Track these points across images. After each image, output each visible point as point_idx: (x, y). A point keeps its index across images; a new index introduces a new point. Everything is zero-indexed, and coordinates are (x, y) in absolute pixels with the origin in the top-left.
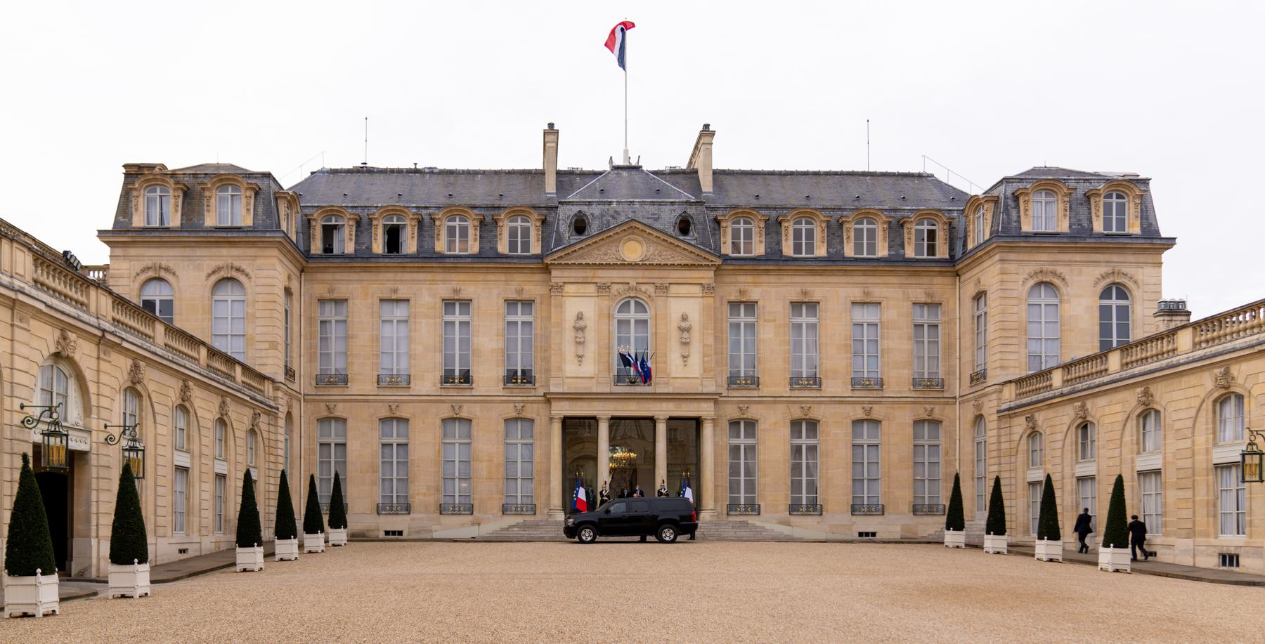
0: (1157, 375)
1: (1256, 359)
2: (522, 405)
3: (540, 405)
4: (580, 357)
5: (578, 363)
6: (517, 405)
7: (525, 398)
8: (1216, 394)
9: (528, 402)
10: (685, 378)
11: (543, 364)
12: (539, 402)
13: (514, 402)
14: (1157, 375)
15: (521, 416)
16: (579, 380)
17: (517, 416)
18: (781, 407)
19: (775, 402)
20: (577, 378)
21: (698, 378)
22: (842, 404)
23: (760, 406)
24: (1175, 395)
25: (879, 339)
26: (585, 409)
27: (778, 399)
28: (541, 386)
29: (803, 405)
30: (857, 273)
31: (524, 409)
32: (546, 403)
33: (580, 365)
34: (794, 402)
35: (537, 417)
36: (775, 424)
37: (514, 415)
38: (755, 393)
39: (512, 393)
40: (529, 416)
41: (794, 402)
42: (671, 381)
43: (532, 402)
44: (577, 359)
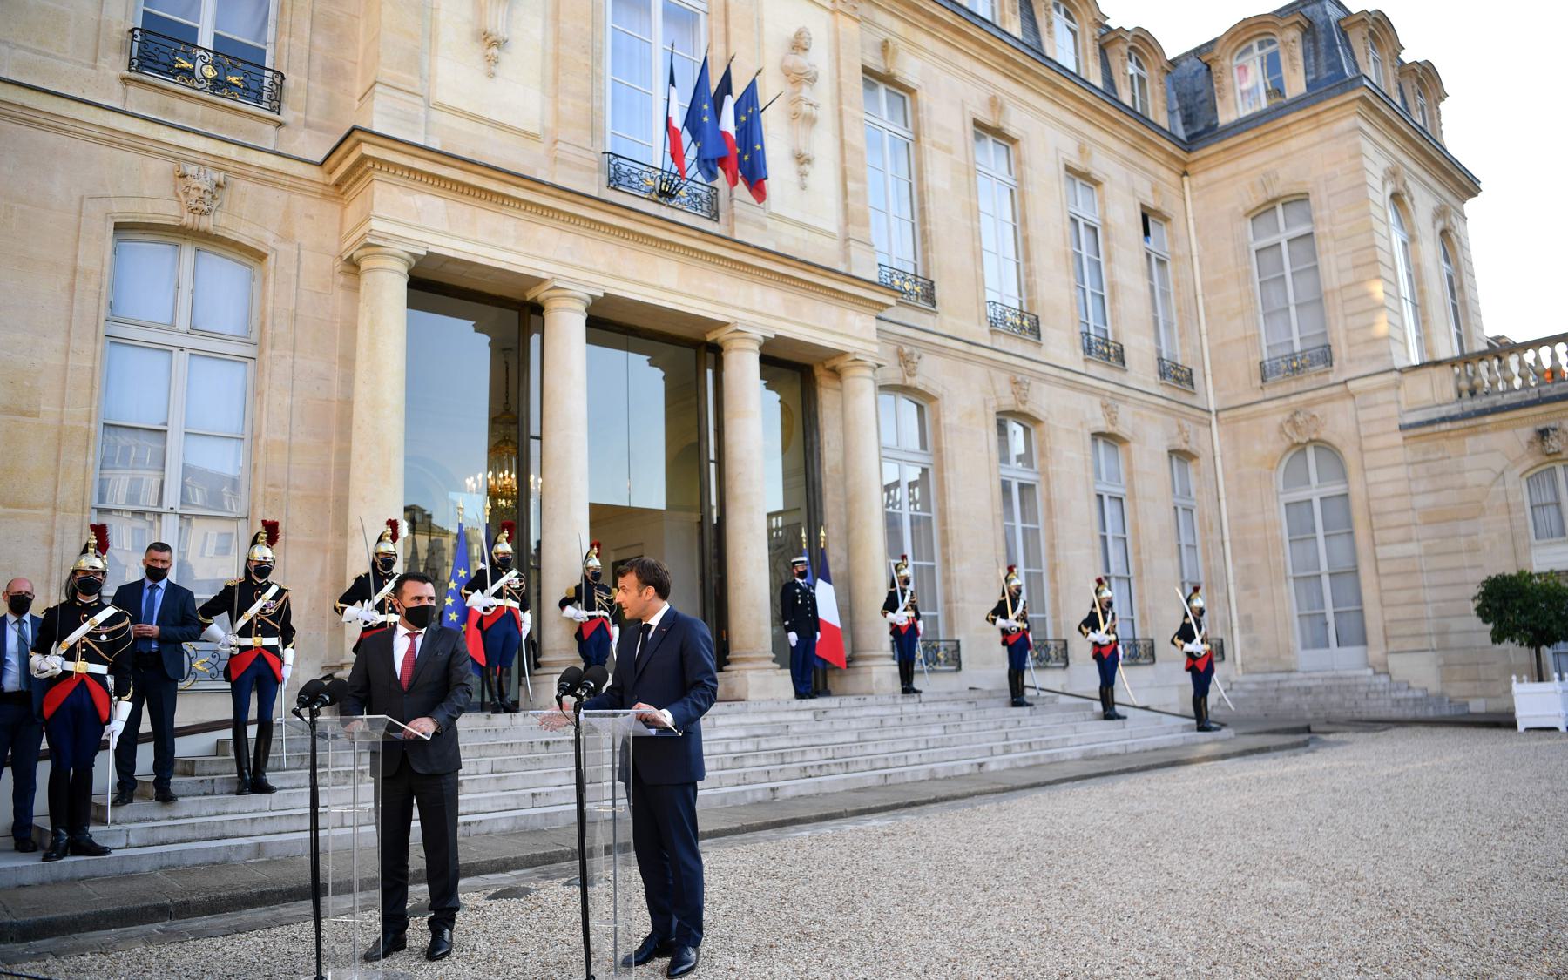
2: (219, 177)
3: (299, 201)
4: (491, 43)
6: (192, 170)
7: (233, 152)
9: (242, 171)
10: (804, 226)
11: (319, 41)
12: (294, 185)
13: (178, 155)
15: (206, 223)
16: (484, 130)
17: (188, 220)
18: (978, 372)
19: (968, 358)
20: (478, 119)
22: (1073, 388)
23: (939, 362)
25: (1102, 259)
26: (510, 245)
27: (975, 350)
28: (307, 125)
31: (225, 195)
33: (492, 75)
34: (1000, 366)
35: (282, 247)
36: (971, 415)
37: (168, 211)
38: (927, 321)
39: (173, 112)
40: (243, 233)
41: (1000, 366)
42: (770, 223)
43: (266, 178)
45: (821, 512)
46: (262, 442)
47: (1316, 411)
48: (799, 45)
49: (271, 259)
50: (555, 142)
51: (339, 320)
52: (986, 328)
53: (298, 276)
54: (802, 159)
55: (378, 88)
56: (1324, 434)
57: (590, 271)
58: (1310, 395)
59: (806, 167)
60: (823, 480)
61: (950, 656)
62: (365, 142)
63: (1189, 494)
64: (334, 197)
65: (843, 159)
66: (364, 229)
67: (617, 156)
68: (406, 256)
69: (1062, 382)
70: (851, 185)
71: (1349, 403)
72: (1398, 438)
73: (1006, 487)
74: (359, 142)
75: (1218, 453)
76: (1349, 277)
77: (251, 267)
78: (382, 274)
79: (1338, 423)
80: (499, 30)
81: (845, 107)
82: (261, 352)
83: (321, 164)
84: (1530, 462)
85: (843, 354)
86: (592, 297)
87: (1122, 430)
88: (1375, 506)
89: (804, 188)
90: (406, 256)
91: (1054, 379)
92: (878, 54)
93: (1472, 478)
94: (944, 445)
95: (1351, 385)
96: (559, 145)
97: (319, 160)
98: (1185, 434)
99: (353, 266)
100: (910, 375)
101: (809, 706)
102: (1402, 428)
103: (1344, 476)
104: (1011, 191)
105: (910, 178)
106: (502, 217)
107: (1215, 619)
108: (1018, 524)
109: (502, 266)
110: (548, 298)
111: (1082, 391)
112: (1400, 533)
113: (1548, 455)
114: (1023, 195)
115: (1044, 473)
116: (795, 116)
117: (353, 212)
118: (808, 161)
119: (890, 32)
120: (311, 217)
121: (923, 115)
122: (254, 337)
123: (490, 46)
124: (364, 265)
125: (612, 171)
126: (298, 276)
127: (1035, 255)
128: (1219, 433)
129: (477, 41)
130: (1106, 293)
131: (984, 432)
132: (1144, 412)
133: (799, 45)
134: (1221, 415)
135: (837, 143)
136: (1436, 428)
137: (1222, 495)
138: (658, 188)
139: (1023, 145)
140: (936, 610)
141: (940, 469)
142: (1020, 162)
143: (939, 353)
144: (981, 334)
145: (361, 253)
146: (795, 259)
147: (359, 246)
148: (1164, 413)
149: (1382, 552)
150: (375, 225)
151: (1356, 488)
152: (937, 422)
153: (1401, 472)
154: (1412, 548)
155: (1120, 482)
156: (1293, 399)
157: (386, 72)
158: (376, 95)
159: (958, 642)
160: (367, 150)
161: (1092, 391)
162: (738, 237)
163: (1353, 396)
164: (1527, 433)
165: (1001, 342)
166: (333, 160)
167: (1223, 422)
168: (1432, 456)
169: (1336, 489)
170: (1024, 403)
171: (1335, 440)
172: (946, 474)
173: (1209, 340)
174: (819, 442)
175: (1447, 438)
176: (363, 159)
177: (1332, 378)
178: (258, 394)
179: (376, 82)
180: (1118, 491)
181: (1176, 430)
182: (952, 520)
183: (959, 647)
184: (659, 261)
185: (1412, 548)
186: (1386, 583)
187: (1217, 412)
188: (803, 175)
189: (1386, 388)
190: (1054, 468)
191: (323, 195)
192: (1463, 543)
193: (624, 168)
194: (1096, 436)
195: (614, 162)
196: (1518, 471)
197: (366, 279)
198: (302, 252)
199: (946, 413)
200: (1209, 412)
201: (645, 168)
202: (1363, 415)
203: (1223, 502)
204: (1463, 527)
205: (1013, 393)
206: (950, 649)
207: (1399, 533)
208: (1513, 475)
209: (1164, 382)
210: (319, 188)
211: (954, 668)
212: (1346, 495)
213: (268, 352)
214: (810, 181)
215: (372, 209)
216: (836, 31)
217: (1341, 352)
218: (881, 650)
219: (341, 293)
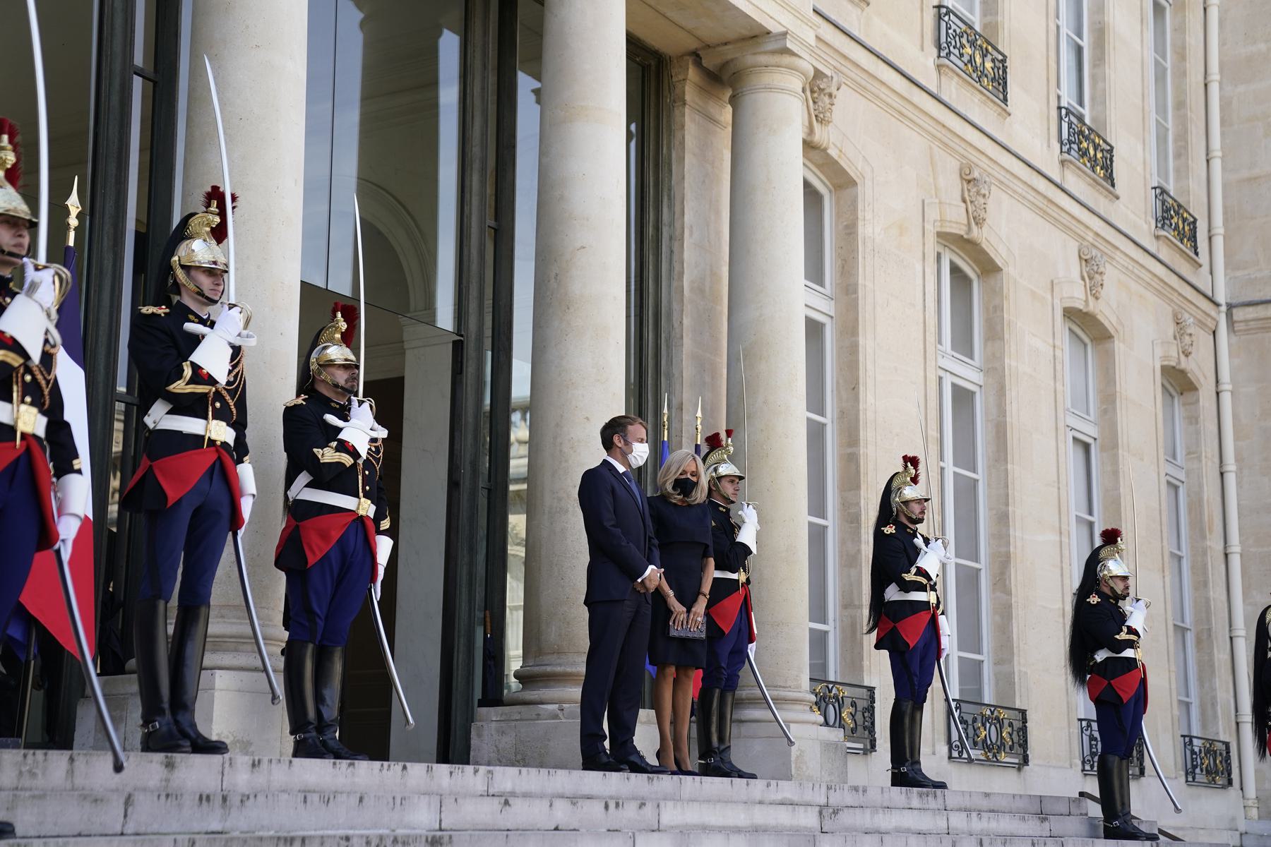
22: (1044, 214)
45: (670, 376)
60: (675, 306)
61: (859, 717)
63: (1174, 457)
69: (1031, 195)
75: (1226, 386)
87: (1105, 311)
91: (1020, 188)
94: (860, 281)
98: (1187, 340)
101: (779, 797)
107: (1214, 705)
108: (950, 469)
111: (1056, 222)
115: (995, 371)
128: (1230, 345)
131: (919, 267)
132: (1134, 286)
134: (1239, 314)
137: (1231, 466)
140: (824, 622)
148: (1159, 293)
152: (849, 230)
155: (1088, 413)
159: (871, 690)
161: (1067, 226)
167: (1237, 327)
172: (861, 341)
173: (1224, 169)
180: (1089, 430)
181: (1171, 329)
183: (872, 699)
187: (1230, 307)
190: (1013, 364)
194: (1071, 314)
199: (869, 216)
200: (1217, 305)
203: (1231, 479)
205: (964, 201)
206: (862, 704)
209: (1162, 233)
211: (861, 746)
218: (799, 686)
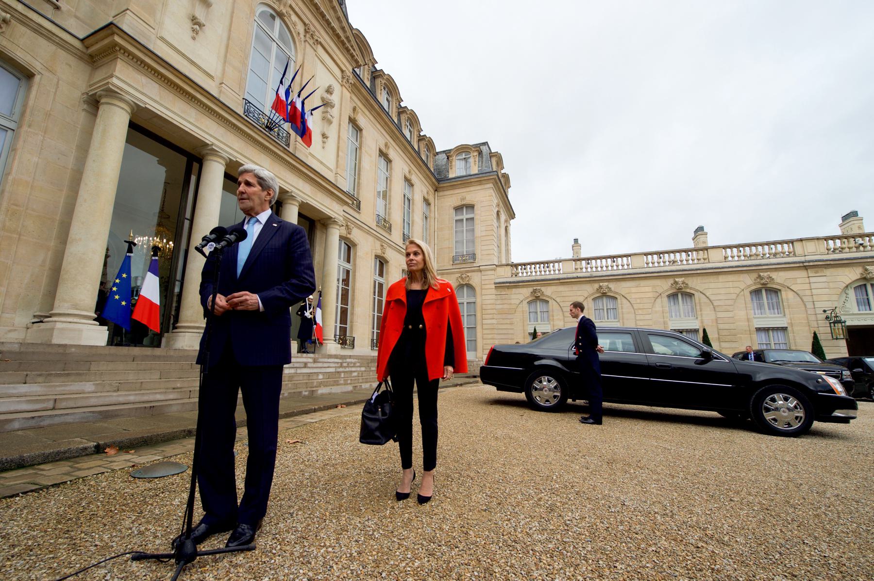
0: (698, 272)
1: (800, 269)
3: (62, 53)
5: (191, 34)
8: (754, 287)
12: (62, 45)
14: (698, 272)
18: (371, 239)
21: (331, 171)
22: (398, 252)
24: (712, 285)
26: (191, 120)
27: (371, 230)
29: (383, 244)
30: (409, 155)
32: (81, 58)
34: (378, 239)
44: (188, 25)
46: (10, 178)
47: (469, 274)
48: (329, 91)
49: (37, 78)
50: (221, 84)
51: (79, 127)
52: (375, 223)
53: (55, 94)
54: (324, 136)
55: (128, 12)
56: (471, 282)
57: (231, 148)
58: (468, 269)
59: (325, 139)
62: (118, 35)
64: (86, 61)
65: (339, 143)
66: (109, 80)
67: (250, 103)
68: (132, 103)
70: (340, 153)
71: (479, 273)
72: (493, 286)
73: (375, 282)
74: (113, 34)
76: (484, 234)
77: (19, 79)
78: (113, 107)
79: (475, 279)
80: (201, 18)
81: (341, 123)
82: (20, 126)
83: (82, 40)
84: (530, 299)
85: (330, 218)
86: (230, 159)
88: (484, 306)
89: (323, 148)
90: (132, 103)
92: (352, 111)
93: (513, 302)
95: (481, 267)
96: (223, 85)
97: (81, 37)
99: (94, 103)
100: (349, 234)
102: (495, 283)
103: (475, 296)
104: (387, 178)
105: (356, 160)
106: (189, 106)
108: (377, 297)
109: (186, 129)
110: (207, 153)
112: (491, 316)
113: (536, 297)
114: (391, 181)
116: (324, 119)
117: (100, 75)
118: (327, 138)
119: (357, 104)
120: (70, 66)
121: (363, 139)
122: (15, 118)
123: (195, 24)
124: (103, 101)
125: (246, 108)
126: (55, 94)
127: (392, 203)
129: (188, 19)
130: (410, 223)
133: (329, 91)
135: (337, 136)
136: (505, 285)
138: (266, 124)
139: (393, 163)
141: (355, 272)
142: (391, 169)
143: (359, 228)
144: (373, 225)
145: (103, 93)
146: (319, 173)
147: (101, 89)
149: (485, 322)
150: (114, 80)
151: (479, 301)
152: (355, 254)
153: (494, 297)
154: (494, 321)
156: (462, 270)
157: (133, 7)
158: (127, 17)
160: (117, 38)
162: (296, 155)
163: (481, 271)
164: (531, 290)
165: (379, 230)
166: (92, 39)
168: (502, 293)
169: (472, 300)
170: (384, 253)
171: (474, 285)
174: (313, 251)
175: (508, 288)
176: (116, 44)
177: (475, 265)
178: (12, 151)
179: (128, 9)
182: (357, 291)
184: (263, 155)
185: (494, 321)
186: (485, 332)
188: (324, 142)
189: (492, 270)
191: (80, 57)
192: (508, 321)
193: (252, 109)
195: (248, 104)
196: (527, 301)
197: (102, 108)
198: (60, 82)
201: (262, 113)
202: (483, 278)
204: (510, 316)
207: (491, 316)
208: (525, 302)
210: (79, 53)
212: (474, 303)
213: (25, 128)
214: (326, 145)
215: (115, 71)
216: (342, 92)
217: (478, 256)
219: (83, 114)
